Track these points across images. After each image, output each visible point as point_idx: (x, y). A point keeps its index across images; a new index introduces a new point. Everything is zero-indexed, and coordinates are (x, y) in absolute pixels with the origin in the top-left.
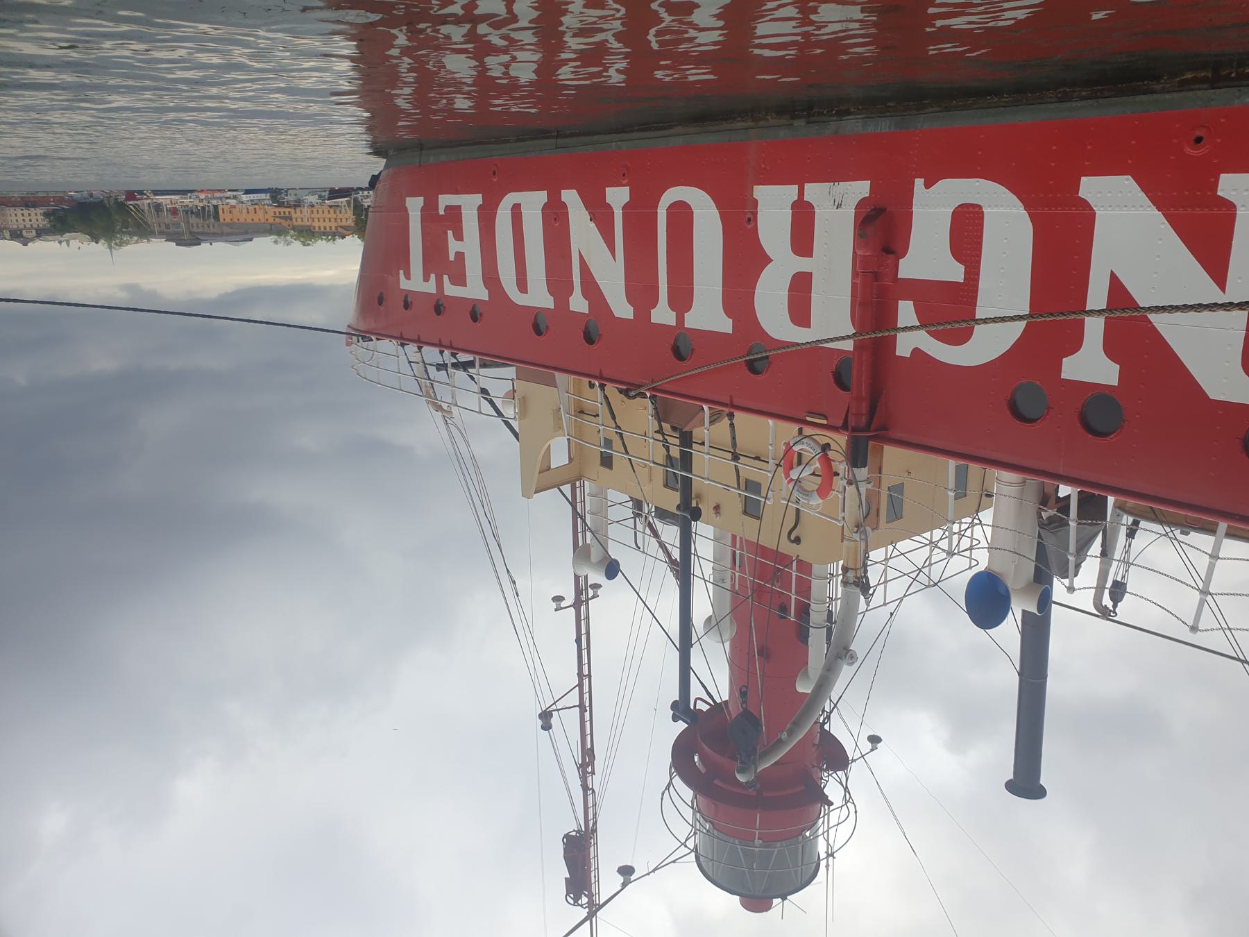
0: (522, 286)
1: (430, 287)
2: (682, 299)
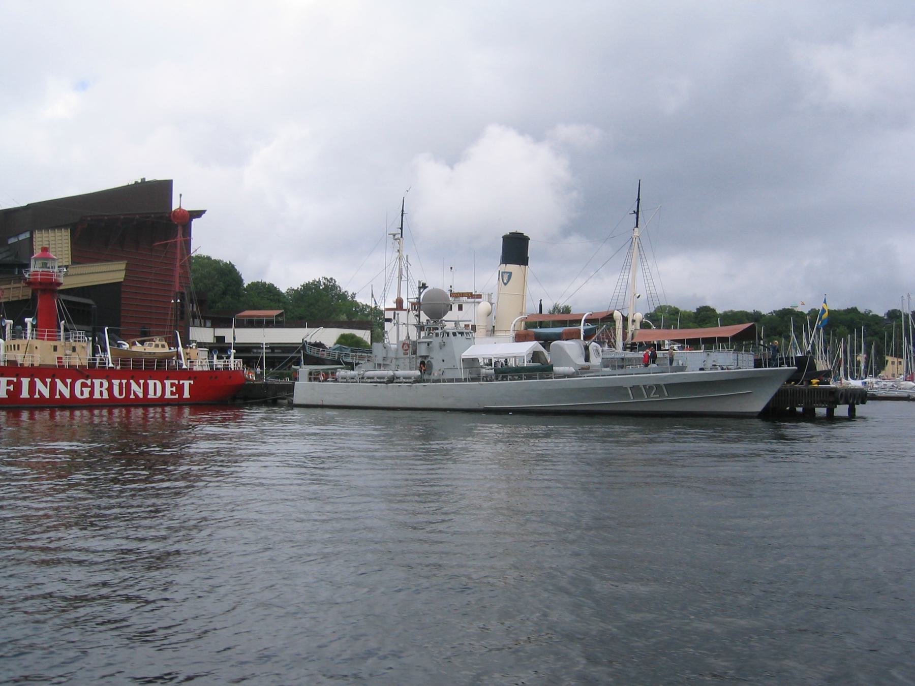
0: (155, 384)
1: (181, 382)
2: (121, 384)
